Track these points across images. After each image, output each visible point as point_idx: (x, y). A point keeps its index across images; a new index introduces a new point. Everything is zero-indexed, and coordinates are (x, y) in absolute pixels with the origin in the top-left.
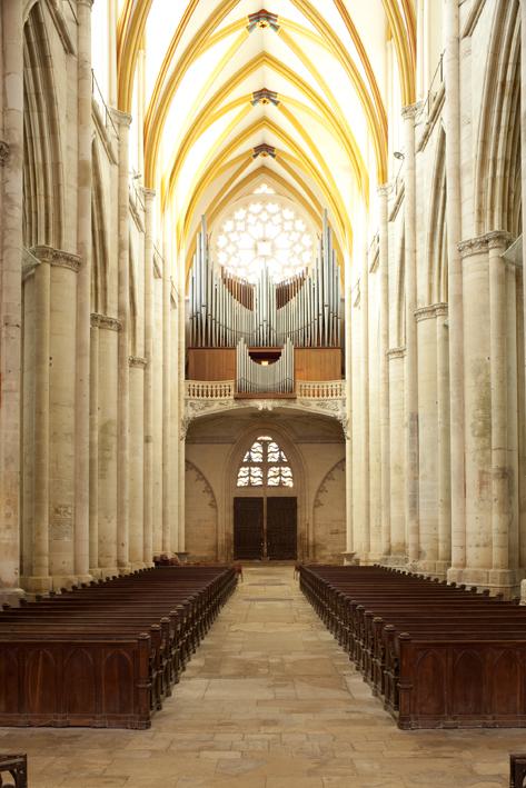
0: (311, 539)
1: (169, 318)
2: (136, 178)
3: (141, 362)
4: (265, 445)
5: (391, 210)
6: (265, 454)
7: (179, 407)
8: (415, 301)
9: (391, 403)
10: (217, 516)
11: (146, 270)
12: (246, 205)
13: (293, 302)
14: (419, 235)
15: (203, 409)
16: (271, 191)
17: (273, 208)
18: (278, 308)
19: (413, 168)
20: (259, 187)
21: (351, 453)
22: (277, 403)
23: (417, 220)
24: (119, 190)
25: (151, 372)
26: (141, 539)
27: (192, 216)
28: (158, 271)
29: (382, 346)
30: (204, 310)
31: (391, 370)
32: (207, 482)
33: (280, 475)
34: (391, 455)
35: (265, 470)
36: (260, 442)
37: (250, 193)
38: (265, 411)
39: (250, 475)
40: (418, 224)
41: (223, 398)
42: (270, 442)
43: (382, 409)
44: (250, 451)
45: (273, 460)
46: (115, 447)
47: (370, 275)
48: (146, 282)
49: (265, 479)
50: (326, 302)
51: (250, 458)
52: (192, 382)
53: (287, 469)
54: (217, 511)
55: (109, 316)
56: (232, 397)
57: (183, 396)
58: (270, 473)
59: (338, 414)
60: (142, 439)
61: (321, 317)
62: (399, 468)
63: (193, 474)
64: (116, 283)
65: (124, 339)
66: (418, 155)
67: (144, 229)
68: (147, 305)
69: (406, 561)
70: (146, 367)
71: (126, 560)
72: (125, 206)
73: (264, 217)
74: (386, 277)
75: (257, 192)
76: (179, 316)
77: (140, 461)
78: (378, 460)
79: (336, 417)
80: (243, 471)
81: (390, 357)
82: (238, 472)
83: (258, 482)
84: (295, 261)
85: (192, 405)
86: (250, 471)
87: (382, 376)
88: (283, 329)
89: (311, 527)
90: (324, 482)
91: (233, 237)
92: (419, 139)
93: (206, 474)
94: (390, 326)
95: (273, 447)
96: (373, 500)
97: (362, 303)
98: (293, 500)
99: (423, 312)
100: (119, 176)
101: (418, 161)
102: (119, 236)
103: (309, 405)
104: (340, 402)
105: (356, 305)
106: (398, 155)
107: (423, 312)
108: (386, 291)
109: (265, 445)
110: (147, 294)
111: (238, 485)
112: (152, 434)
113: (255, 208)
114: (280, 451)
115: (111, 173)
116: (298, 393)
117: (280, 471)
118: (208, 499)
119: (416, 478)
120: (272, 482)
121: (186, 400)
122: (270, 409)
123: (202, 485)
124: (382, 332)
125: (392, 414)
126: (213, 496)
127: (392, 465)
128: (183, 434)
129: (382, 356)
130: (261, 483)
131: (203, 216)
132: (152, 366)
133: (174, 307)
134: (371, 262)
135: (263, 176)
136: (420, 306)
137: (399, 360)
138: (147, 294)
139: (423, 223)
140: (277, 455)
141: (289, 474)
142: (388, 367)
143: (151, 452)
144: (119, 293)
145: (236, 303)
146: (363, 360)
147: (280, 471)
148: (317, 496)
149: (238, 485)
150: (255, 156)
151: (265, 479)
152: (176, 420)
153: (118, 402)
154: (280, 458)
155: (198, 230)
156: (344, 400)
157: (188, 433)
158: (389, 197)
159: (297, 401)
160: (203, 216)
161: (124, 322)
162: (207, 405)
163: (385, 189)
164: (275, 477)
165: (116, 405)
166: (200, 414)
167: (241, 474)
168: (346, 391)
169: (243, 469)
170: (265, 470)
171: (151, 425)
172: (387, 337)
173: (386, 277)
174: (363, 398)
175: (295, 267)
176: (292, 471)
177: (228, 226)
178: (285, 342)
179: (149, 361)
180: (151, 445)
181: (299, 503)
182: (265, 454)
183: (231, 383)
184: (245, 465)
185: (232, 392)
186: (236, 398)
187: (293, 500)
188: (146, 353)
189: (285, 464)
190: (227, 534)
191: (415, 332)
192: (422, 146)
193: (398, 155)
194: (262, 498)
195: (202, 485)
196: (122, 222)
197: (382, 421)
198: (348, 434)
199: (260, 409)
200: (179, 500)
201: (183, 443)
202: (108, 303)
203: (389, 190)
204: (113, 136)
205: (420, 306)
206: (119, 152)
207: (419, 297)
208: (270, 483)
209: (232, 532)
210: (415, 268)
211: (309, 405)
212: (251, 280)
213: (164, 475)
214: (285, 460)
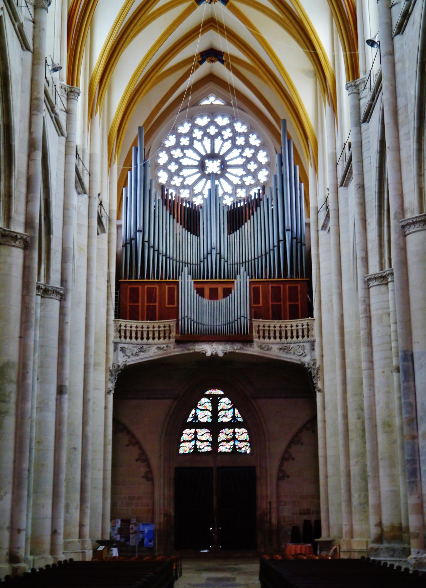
0: (274, 520)
1: (95, 239)
2: (55, 70)
3: (55, 291)
4: (215, 400)
5: (364, 109)
6: (215, 412)
7: (107, 353)
8: (402, 210)
9: (376, 341)
10: (153, 493)
11: (66, 180)
12: (191, 119)
13: (247, 226)
14: (402, 131)
15: (136, 355)
16: (219, 102)
17: (222, 121)
18: (229, 233)
19: (392, 53)
20: (207, 98)
21: (324, 408)
22: (229, 348)
23: (400, 112)
24: (32, 80)
25: (69, 304)
26: (48, 523)
27: (127, 126)
28: (82, 184)
29: (360, 271)
30: (139, 236)
31: (373, 300)
32: (141, 448)
33: (234, 439)
34: (378, 408)
35: (215, 434)
36: (208, 396)
37: (196, 103)
38: (214, 357)
39: (195, 439)
40: (401, 118)
41: (162, 340)
42: (222, 397)
43: (363, 350)
44: (196, 408)
45: (226, 420)
46: (13, 398)
47: (340, 189)
48: (66, 194)
49: (215, 444)
50: (288, 224)
51: (196, 417)
52: (123, 322)
53: (243, 430)
54: (153, 484)
55: (13, 230)
56: (173, 340)
57: (112, 339)
58: (222, 437)
59: (307, 360)
60: (53, 389)
61: (281, 244)
62: (388, 425)
63: (124, 438)
64: (23, 190)
65: (32, 259)
66: (397, 38)
67: (65, 133)
68: (65, 222)
69: (407, 552)
70: (63, 298)
71: (22, 553)
72: (38, 99)
73: (212, 130)
74: (362, 187)
75: (206, 102)
76: (109, 242)
77: (51, 417)
78: (360, 417)
79: (303, 364)
80: (187, 434)
81: (371, 284)
82: (182, 434)
83: (206, 448)
84: (249, 180)
85: (122, 349)
86: (196, 433)
87: (361, 307)
88: (236, 258)
89: (274, 505)
90: (289, 446)
91: (177, 153)
92: (397, 18)
93: (139, 435)
94: (370, 246)
95: (225, 402)
96: (355, 469)
97: (331, 223)
98: (252, 469)
99: (413, 223)
100: (33, 64)
101: (397, 45)
102: (30, 133)
103: (269, 349)
104: (307, 346)
105: (324, 227)
106: (371, 43)
107: (413, 223)
108: (363, 204)
109: (215, 400)
110: (66, 208)
111: (181, 451)
112: (67, 383)
113: (202, 121)
114: (233, 408)
115: (22, 59)
116: (255, 334)
117: (234, 433)
118: (143, 470)
119: (414, 437)
120: (224, 448)
121: (116, 344)
122: (221, 354)
123: (134, 451)
124: (360, 254)
125: (376, 356)
126: (149, 466)
127: (379, 422)
128: (111, 386)
129: (361, 285)
130: (209, 449)
131: (140, 128)
132: (70, 297)
133: (103, 231)
134: (340, 174)
135: (211, 86)
136: (408, 216)
137: (383, 288)
138: (66, 208)
139: (407, 117)
140: (230, 414)
141: (246, 436)
142: (369, 297)
143: (66, 405)
144: (28, 202)
145: (179, 228)
146: (335, 291)
147: (234, 433)
148: (281, 465)
149: (181, 451)
150: (201, 62)
151: (215, 444)
152: (102, 368)
153: (20, 337)
154: (234, 417)
155: (135, 144)
156: (312, 343)
157: (117, 385)
158: (362, 95)
159: (255, 345)
160: (140, 128)
161: (32, 238)
162: (141, 350)
163: (357, 86)
164: (228, 441)
165: (17, 339)
166: (132, 360)
167: (185, 437)
168: (316, 332)
169: (187, 431)
170: (215, 434)
171: (67, 372)
172: (366, 260)
173: (362, 187)
174: (337, 338)
175: (251, 186)
176: (249, 433)
177: (171, 141)
178: (238, 272)
179: (66, 291)
180: (66, 397)
181: (258, 473)
182: (215, 412)
183: (172, 323)
184: (191, 426)
185: (174, 334)
186: (178, 342)
187: (252, 469)
188: (63, 281)
189: (240, 425)
190: (166, 515)
191: (403, 249)
192: (401, 28)
193: (371, 43)
194: (211, 468)
195: (134, 451)
196: (34, 117)
197: (364, 365)
198: (319, 385)
199: (208, 354)
200: (105, 471)
201: (111, 397)
202: (13, 214)
203: (362, 86)
204: (27, 19)
205: (408, 216)
206: (34, 39)
207: (406, 205)
208: (222, 449)
209: (172, 512)
210: (399, 170)
211: (269, 349)
212: (198, 201)
213: (84, 437)
214: (240, 420)
